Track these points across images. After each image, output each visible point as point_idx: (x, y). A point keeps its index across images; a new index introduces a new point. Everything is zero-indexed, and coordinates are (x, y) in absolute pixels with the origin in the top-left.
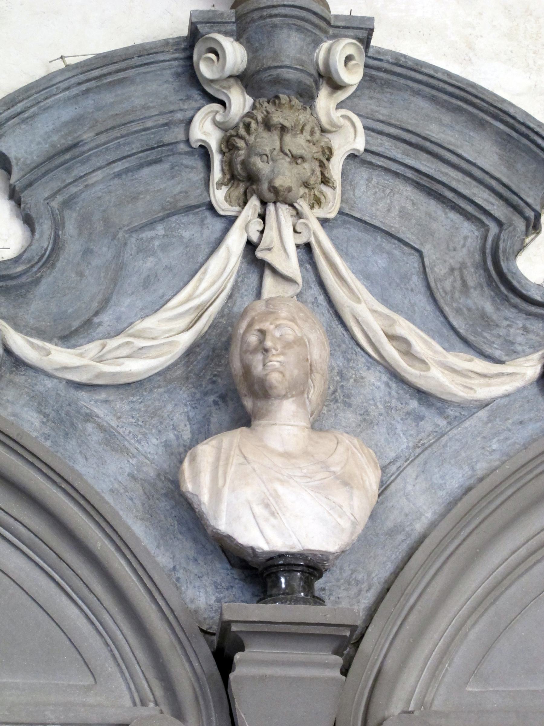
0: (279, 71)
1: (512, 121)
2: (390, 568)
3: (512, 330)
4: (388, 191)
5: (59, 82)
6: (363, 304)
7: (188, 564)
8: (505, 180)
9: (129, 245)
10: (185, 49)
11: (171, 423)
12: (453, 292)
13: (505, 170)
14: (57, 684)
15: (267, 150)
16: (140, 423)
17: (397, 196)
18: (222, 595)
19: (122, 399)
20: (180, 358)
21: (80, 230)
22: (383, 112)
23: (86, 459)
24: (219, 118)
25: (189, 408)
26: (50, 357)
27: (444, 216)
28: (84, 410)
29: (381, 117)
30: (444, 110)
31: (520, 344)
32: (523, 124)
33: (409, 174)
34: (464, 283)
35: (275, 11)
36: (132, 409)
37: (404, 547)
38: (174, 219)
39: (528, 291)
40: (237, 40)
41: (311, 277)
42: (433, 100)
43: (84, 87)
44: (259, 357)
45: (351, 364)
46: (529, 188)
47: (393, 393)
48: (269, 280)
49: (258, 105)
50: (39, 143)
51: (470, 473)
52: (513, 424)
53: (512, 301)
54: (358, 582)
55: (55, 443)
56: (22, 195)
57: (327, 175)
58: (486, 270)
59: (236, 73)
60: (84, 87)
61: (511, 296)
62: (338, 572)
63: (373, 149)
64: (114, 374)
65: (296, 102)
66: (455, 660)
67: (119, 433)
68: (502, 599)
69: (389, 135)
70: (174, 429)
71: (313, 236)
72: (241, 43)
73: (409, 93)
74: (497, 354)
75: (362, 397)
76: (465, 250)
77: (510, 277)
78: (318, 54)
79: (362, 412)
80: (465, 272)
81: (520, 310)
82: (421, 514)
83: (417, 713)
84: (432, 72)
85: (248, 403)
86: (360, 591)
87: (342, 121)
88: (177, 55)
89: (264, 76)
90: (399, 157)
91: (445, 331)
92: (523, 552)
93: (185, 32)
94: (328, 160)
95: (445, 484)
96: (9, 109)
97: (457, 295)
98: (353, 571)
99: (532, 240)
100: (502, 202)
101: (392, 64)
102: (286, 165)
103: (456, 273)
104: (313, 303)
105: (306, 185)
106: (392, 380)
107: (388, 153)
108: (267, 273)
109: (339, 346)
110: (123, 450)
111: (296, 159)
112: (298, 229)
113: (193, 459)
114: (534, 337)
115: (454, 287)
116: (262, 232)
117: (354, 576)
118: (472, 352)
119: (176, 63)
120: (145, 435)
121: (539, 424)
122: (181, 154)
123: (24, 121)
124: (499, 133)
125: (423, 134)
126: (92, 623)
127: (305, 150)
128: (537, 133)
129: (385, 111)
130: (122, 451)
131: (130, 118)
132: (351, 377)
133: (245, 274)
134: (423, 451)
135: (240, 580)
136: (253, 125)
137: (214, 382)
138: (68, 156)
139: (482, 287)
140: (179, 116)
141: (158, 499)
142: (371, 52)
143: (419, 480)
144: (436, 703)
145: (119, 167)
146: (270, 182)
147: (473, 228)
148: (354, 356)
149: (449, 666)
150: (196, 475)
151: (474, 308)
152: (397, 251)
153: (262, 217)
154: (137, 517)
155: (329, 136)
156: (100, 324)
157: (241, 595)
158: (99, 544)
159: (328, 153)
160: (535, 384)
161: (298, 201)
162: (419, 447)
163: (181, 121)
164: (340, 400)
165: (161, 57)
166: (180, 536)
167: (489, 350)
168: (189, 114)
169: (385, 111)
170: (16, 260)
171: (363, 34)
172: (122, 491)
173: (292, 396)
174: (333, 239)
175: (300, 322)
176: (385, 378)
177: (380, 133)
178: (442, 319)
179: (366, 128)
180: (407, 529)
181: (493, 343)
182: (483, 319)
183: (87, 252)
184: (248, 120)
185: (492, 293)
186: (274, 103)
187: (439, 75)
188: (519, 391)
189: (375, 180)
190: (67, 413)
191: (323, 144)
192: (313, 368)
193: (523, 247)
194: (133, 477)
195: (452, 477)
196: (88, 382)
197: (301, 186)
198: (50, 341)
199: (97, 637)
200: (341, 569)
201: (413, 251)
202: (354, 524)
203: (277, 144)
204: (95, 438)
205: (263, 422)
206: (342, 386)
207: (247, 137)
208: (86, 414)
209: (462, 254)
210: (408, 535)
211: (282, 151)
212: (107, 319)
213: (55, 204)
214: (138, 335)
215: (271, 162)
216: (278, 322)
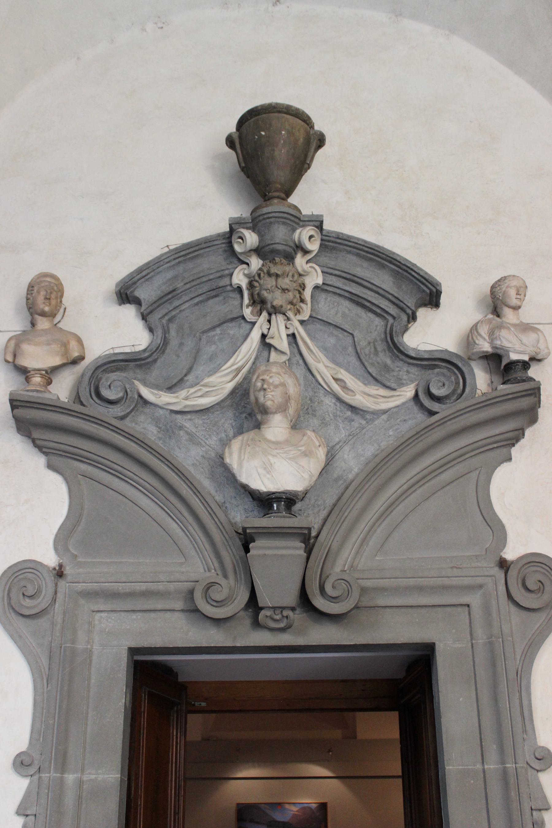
0: (274, 246)
1: (399, 264)
2: (335, 498)
3: (401, 373)
4: (336, 304)
5: (164, 259)
7: (231, 499)
8: (396, 295)
9: (202, 340)
10: (228, 238)
11: (223, 429)
12: (370, 355)
13: (396, 290)
14: (166, 562)
15: (269, 286)
16: (207, 430)
17: (340, 306)
18: (248, 515)
19: (198, 418)
20: (228, 395)
21: (178, 333)
22: (332, 264)
23: (180, 449)
24: (246, 272)
25: (233, 421)
26: (161, 398)
27: (365, 315)
28: (179, 424)
29: (331, 266)
30: (363, 260)
31: (405, 380)
32: (405, 265)
33: (347, 294)
35: (271, 215)
36: (204, 423)
37: (343, 486)
38: (225, 325)
39: (408, 352)
40: (253, 231)
41: (296, 351)
42: (358, 255)
43: (177, 261)
44: (262, 393)
45: (316, 394)
46: (409, 298)
47: (338, 408)
48: (273, 354)
49: (265, 264)
50: (155, 291)
51: (378, 448)
52: (401, 421)
53: (400, 357)
54: (318, 506)
55: (164, 442)
56: (147, 317)
57: (303, 298)
58: (387, 342)
59: (253, 248)
60: (177, 261)
61: (400, 355)
62: (308, 501)
64: (194, 406)
65: (284, 261)
66: (370, 543)
67: (196, 435)
68: (394, 512)
69: (336, 275)
70: (225, 432)
71: (296, 330)
72: (255, 233)
73: (345, 252)
74: (393, 385)
75: (322, 411)
76: (376, 332)
77: (398, 345)
78: (295, 236)
79: (321, 419)
80: (376, 344)
81: (405, 362)
82: (352, 470)
83: (348, 572)
84: (356, 241)
85: (259, 417)
86: (319, 510)
87: (310, 269)
88: (224, 241)
89: (267, 249)
90: (341, 286)
91: (365, 374)
92: (405, 487)
93: (228, 229)
94: (304, 290)
95: (364, 454)
96: (139, 274)
97: (372, 356)
98: (316, 500)
99: (412, 325)
100: (395, 306)
101: (336, 238)
102: (279, 294)
103: (372, 344)
104: (297, 364)
105: (291, 303)
106: (337, 402)
107: (335, 285)
108: (272, 349)
109: (310, 385)
110: (199, 444)
111: (284, 290)
112: (288, 327)
113: (230, 447)
114: (412, 376)
115: (370, 352)
116: (269, 329)
117: (316, 503)
118: (380, 385)
119: (224, 245)
120: (210, 435)
121: (414, 421)
122: (228, 291)
123: (147, 280)
124: (392, 270)
125: (353, 273)
126: (184, 531)
127: (289, 286)
128: (412, 269)
129: (333, 263)
130: (198, 444)
131: (202, 275)
132: (316, 401)
133: (262, 351)
134: (353, 438)
135: (258, 507)
136: (262, 275)
137: (245, 407)
138: (170, 296)
139: (385, 351)
140: (227, 272)
141: (216, 467)
142: (324, 233)
144: (359, 566)
146: (271, 303)
148: (318, 390)
149: (366, 547)
150: (231, 454)
151: (380, 362)
152: (341, 335)
153: (269, 321)
154: (205, 477)
155: (304, 278)
156: (187, 381)
157: (258, 514)
158: (185, 491)
159: (303, 286)
160: (412, 400)
161: (288, 312)
162: (351, 435)
163: (228, 275)
164: (310, 413)
165: (216, 243)
166: (227, 486)
167: (388, 384)
168: (231, 271)
169: (333, 263)
170: (145, 351)
171: (318, 224)
172: (198, 464)
173: (279, 412)
175: (282, 374)
176: (334, 401)
177: (331, 274)
178: (364, 369)
179: (322, 272)
181: (391, 380)
182: (386, 367)
183: (181, 344)
184: (259, 272)
185: (390, 354)
186: (273, 263)
187: (360, 242)
188: (403, 404)
189: (329, 299)
190: (171, 426)
191: (300, 282)
192: (290, 397)
193: (406, 329)
194: (203, 457)
195: (368, 450)
196: (181, 410)
197: (288, 304)
198: (162, 390)
199: (186, 538)
200: (310, 499)
201: (349, 335)
202: (311, 476)
203: (274, 283)
204: (184, 438)
205: (265, 426)
206: (311, 406)
207: (259, 281)
208: (180, 426)
209: (374, 335)
210: (345, 481)
211: (277, 287)
212: (191, 378)
213: (164, 321)
214: (205, 385)
215: (271, 293)
216: (271, 375)
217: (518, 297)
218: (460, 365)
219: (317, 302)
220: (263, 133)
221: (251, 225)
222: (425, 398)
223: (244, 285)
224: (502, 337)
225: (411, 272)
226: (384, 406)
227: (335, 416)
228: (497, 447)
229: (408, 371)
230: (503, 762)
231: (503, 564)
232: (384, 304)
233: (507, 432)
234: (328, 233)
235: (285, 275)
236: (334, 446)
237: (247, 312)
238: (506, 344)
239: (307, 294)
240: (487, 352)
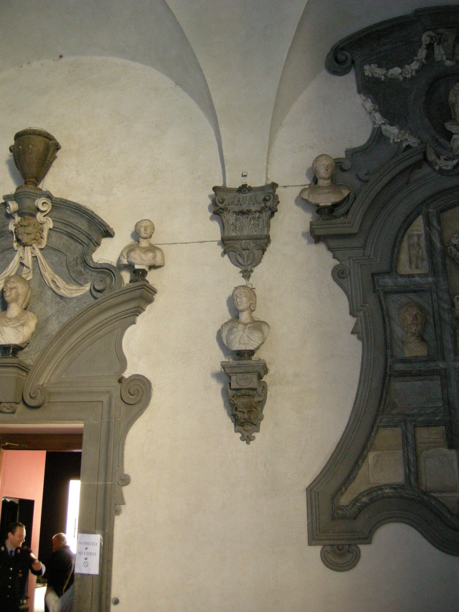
6: (47, 272)
8: (88, 232)
12: (73, 266)
33: (65, 232)
35: (21, 194)
42: (71, 211)
63: (55, 226)
65: (30, 217)
74: (82, 283)
81: (90, 270)
84: (69, 203)
90: (62, 228)
94: (43, 232)
98: (36, 347)
103: (75, 260)
124: (86, 218)
143: (56, 321)
167: (80, 282)
173: (13, 302)
174: (42, 254)
179: (53, 221)
180: (51, 334)
181: (81, 280)
206: (41, 296)
217: (145, 232)
218: (114, 272)
219: (51, 237)
220: (20, 147)
221: (14, 198)
222: (94, 291)
223: (13, 232)
224: (131, 256)
225: (95, 219)
226: (75, 295)
228: (128, 317)
229: (91, 275)
230: (106, 481)
231: (121, 380)
232: (83, 237)
233: (131, 309)
234: (56, 199)
235: (29, 225)
236: (49, 317)
237: (15, 245)
239: (45, 234)
240: (125, 264)
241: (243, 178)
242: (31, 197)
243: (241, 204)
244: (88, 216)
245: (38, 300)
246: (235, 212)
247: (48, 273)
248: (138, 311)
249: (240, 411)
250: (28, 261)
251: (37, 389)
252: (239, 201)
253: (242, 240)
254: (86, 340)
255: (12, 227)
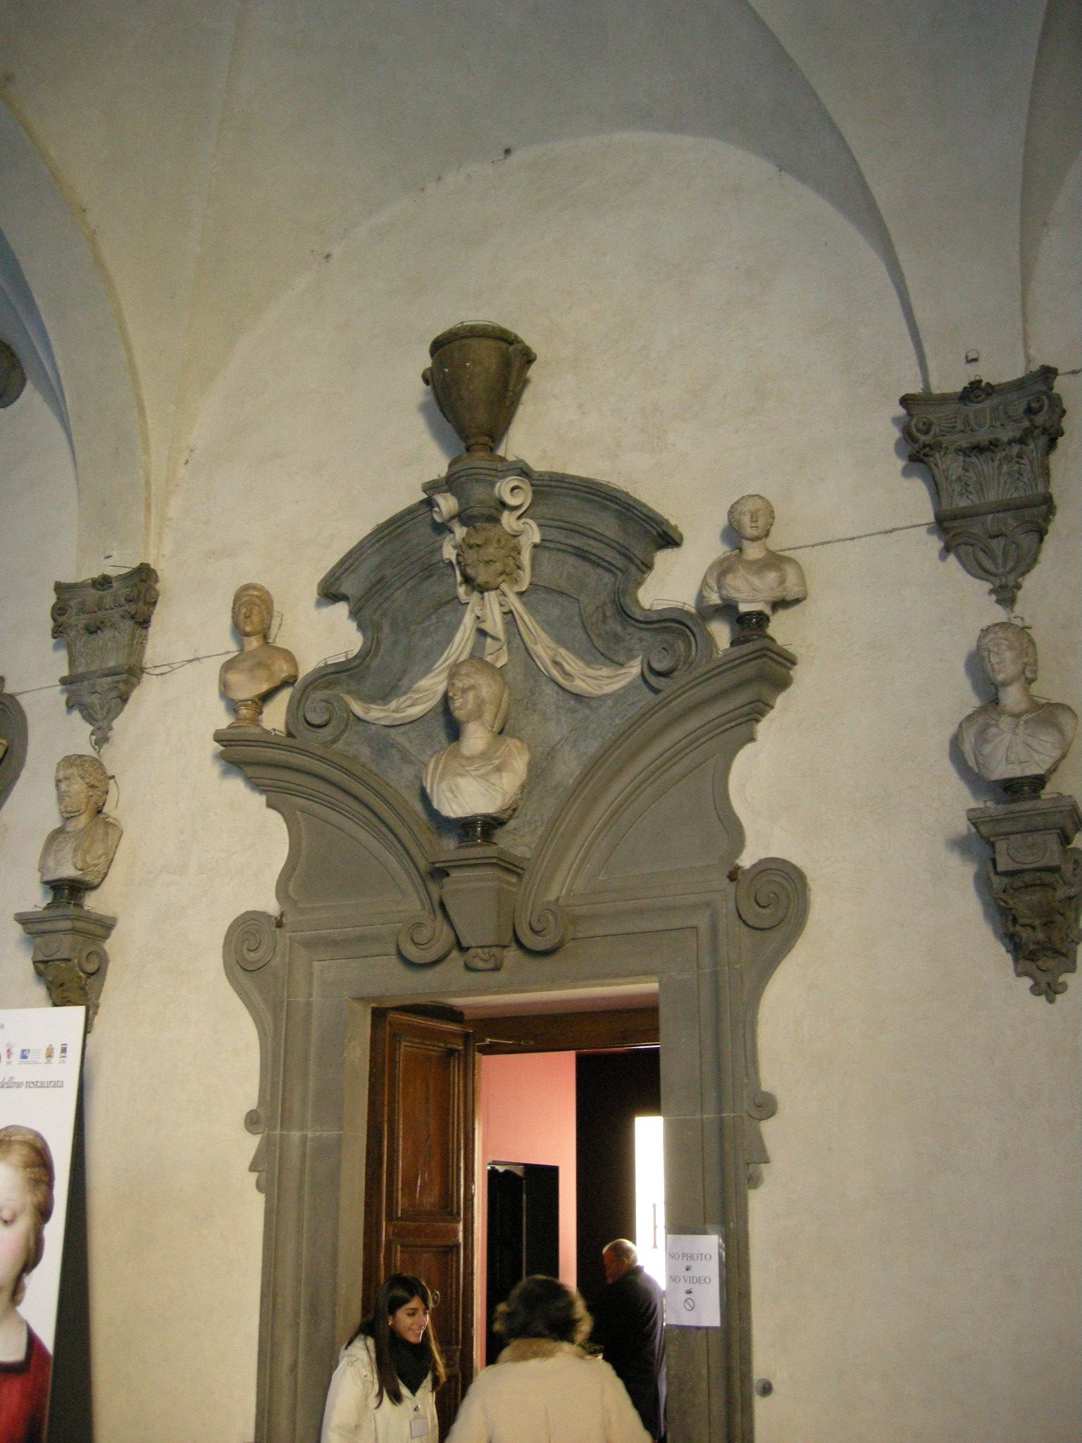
6: (539, 645)
8: (621, 541)
13: (621, 534)
28: (391, 741)
33: (570, 549)
34: (604, 615)
35: (459, 475)
43: (381, 542)
54: (535, 821)
63: (544, 538)
65: (486, 525)
74: (621, 660)
76: (606, 593)
90: (563, 540)
94: (519, 554)
103: (600, 609)
124: (616, 510)
138: (379, 586)
145: (409, 585)
147: (610, 576)
165: (420, 512)
167: (616, 659)
174: (524, 604)
177: (550, 526)
179: (540, 526)
183: (395, 643)
187: (575, 482)
217: (754, 525)
220: (446, 370)
221: (446, 487)
223: (454, 561)
226: (608, 689)
227: (558, 707)
230: (720, 1110)
231: (734, 875)
232: (611, 555)
233: (742, 707)
234: (541, 476)
235: (487, 542)
237: (461, 590)
238: (733, 594)
239: (526, 558)
240: (716, 605)
241: (970, 367)
242: (483, 477)
243: (972, 430)
244: (617, 504)
245: (527, 709)
246: (960, 450)
247: (543, 647)
248: (758, 710)
249: (1023, 926)
250: (495, 624)
251: (545, 911)
252: (966, 422)
253: (985, 514)
254: (645, 789)
255: (449, 553)
